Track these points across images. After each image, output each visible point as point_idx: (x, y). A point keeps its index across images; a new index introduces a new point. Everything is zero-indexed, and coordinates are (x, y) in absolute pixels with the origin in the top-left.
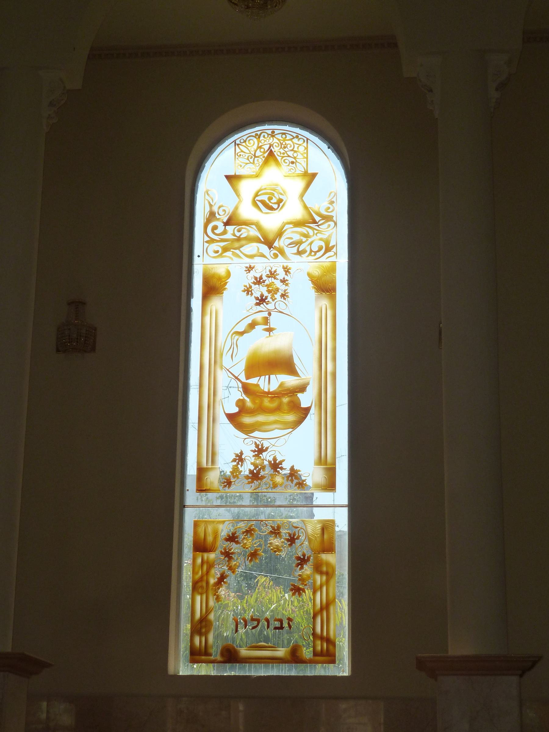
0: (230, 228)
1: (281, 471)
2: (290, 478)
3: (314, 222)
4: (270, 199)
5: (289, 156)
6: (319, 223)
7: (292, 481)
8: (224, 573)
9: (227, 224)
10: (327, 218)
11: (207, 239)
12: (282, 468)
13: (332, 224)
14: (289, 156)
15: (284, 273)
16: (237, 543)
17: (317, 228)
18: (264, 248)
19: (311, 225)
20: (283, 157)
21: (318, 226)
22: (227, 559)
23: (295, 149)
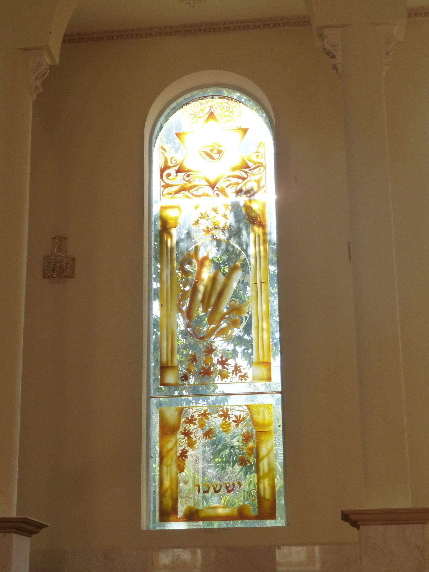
0: (181, 175)
1: (227, 367)
2: (235, 372)
3: (248, 167)
4: (212, 150)
5: (225, 116)
6: (251, 168)
7: (236, 374)
8: (184, 449)
9: (178, 172)
10: (259, 165)
11: (163, 184)
12: (228, 365)
13: (262, 168)
14: (225, 116)
15: (225, 209)
16: (195, 424)
17: (250, 171)
18: (209, 190)
19: (246, 170)
20: (221, 116)
21: (251, 170)
22: (186, 438)
23: (231, 110)
